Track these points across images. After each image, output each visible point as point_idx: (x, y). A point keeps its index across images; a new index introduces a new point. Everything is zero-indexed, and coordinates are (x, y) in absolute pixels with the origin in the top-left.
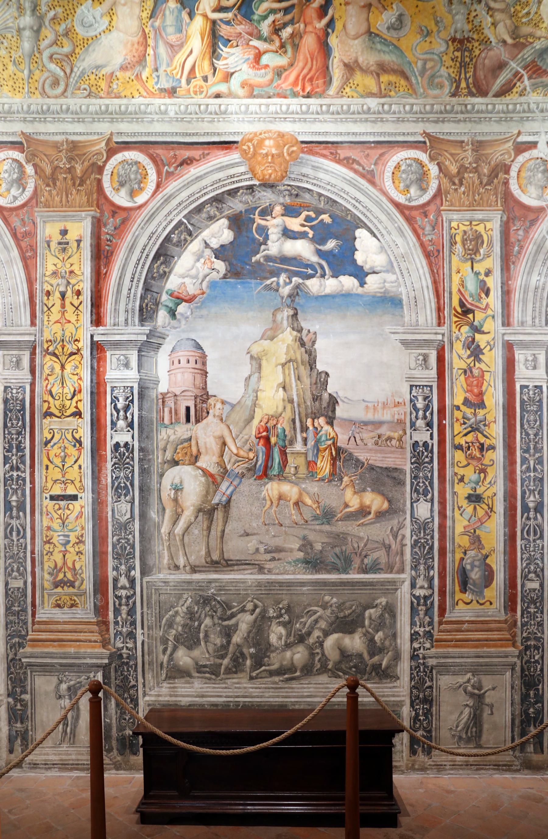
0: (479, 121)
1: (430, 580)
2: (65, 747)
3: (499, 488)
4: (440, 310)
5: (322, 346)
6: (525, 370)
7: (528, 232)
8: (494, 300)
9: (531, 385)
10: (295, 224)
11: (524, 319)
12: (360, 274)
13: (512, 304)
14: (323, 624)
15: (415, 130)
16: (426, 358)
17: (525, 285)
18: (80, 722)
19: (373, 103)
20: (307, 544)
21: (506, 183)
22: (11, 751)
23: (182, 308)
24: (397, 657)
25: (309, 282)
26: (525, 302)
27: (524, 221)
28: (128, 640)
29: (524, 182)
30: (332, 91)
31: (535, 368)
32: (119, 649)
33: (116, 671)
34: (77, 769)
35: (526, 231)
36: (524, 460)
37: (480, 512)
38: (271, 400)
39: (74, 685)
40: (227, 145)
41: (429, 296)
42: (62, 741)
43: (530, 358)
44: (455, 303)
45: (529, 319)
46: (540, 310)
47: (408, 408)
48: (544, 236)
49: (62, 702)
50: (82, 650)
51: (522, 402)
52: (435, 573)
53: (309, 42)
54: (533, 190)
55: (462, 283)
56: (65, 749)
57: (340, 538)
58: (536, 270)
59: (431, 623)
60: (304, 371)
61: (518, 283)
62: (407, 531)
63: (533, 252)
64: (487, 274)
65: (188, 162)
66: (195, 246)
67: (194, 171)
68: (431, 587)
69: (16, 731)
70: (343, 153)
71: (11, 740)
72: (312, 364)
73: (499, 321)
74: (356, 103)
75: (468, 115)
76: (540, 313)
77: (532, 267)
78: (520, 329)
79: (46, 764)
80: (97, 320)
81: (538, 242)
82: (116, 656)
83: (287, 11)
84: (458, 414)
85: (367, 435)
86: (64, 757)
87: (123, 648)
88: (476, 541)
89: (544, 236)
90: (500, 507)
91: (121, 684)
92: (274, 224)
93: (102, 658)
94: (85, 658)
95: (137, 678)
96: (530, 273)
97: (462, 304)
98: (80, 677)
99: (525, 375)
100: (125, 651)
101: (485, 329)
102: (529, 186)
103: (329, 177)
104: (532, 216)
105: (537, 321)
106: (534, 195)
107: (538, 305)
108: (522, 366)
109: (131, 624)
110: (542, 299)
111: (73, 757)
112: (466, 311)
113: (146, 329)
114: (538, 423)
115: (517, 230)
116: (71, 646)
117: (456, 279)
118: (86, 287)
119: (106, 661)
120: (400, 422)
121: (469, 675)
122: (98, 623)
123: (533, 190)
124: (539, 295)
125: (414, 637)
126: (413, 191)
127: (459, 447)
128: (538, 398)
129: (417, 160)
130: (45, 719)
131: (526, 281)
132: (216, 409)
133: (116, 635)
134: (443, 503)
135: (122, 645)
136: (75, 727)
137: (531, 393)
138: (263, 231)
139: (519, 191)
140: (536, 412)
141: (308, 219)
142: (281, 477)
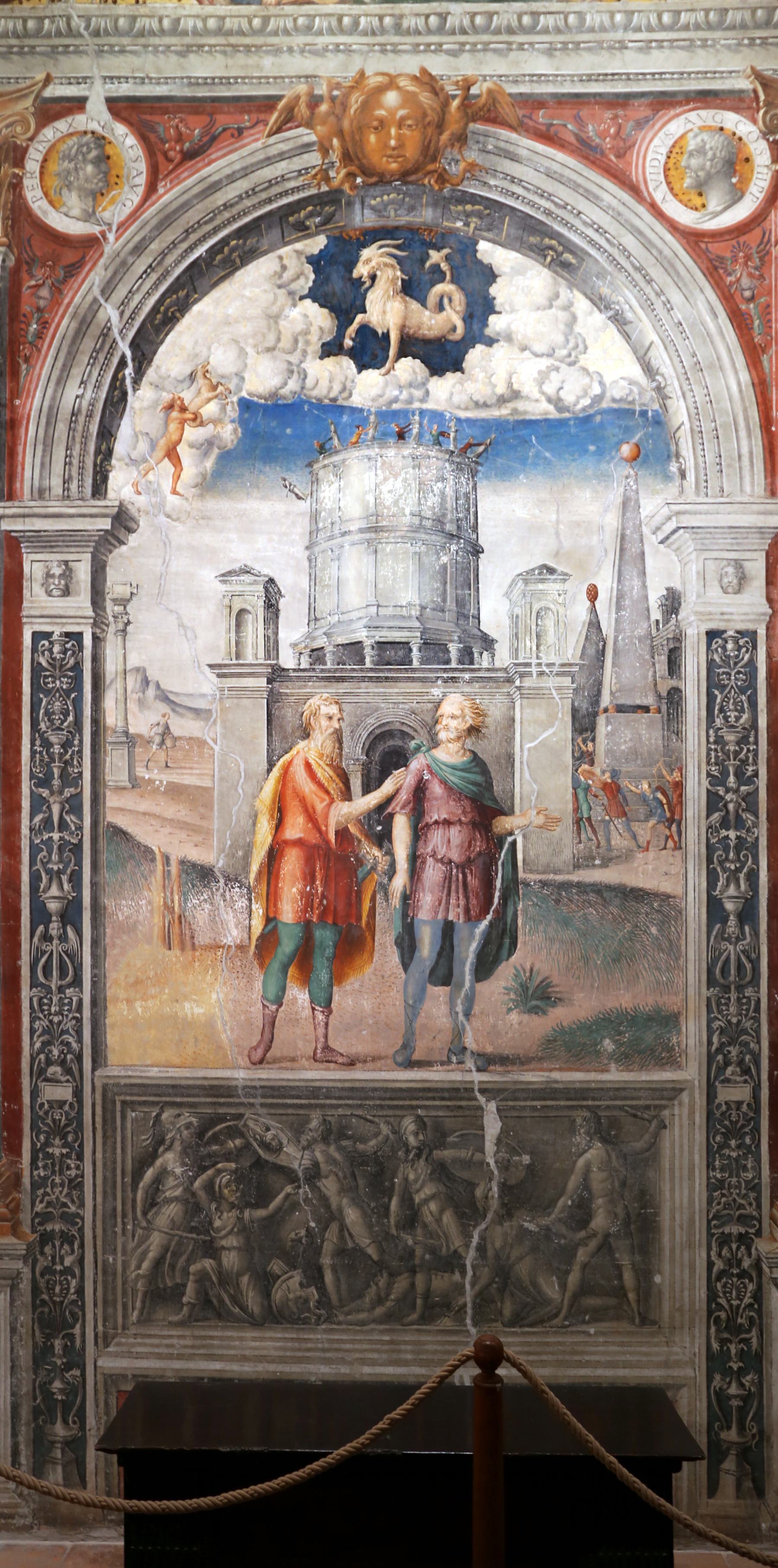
6: (43, 597)
7: (60, 291)
9: (57, 630)
11: (46, 483)
13: (20, 449)
17: (51, 408)
26: (48, 444)
27: (52, 268)
29: (53, 183)
31: (66, 592)
35: (57, 291)
36: (38, 803)
43: (57, 571)
45: (56, 483)
46: (82, 462)
48: (95, 300)
51: (36, 668)
54: (74, 202)
58: (77, 373)
63: (71, 333)
76: (82, 468)
77: (67, 369)
78: (37, 507)
81: (82, 312)
89: (95, 300)
96: (62, 382)
102: (65, 191)
104: (70, 257)
105: (74, 486)
106: (76, 212)
107: (76, 452)
108: (38, 589)
110: (85, 437)
114: (71, 718)
115: (38, 286)
124: (80, 428)
128: (72, 661)
131: (53, 398)
137: (56, 649)
139: (44, 204)
140: (68, 693)
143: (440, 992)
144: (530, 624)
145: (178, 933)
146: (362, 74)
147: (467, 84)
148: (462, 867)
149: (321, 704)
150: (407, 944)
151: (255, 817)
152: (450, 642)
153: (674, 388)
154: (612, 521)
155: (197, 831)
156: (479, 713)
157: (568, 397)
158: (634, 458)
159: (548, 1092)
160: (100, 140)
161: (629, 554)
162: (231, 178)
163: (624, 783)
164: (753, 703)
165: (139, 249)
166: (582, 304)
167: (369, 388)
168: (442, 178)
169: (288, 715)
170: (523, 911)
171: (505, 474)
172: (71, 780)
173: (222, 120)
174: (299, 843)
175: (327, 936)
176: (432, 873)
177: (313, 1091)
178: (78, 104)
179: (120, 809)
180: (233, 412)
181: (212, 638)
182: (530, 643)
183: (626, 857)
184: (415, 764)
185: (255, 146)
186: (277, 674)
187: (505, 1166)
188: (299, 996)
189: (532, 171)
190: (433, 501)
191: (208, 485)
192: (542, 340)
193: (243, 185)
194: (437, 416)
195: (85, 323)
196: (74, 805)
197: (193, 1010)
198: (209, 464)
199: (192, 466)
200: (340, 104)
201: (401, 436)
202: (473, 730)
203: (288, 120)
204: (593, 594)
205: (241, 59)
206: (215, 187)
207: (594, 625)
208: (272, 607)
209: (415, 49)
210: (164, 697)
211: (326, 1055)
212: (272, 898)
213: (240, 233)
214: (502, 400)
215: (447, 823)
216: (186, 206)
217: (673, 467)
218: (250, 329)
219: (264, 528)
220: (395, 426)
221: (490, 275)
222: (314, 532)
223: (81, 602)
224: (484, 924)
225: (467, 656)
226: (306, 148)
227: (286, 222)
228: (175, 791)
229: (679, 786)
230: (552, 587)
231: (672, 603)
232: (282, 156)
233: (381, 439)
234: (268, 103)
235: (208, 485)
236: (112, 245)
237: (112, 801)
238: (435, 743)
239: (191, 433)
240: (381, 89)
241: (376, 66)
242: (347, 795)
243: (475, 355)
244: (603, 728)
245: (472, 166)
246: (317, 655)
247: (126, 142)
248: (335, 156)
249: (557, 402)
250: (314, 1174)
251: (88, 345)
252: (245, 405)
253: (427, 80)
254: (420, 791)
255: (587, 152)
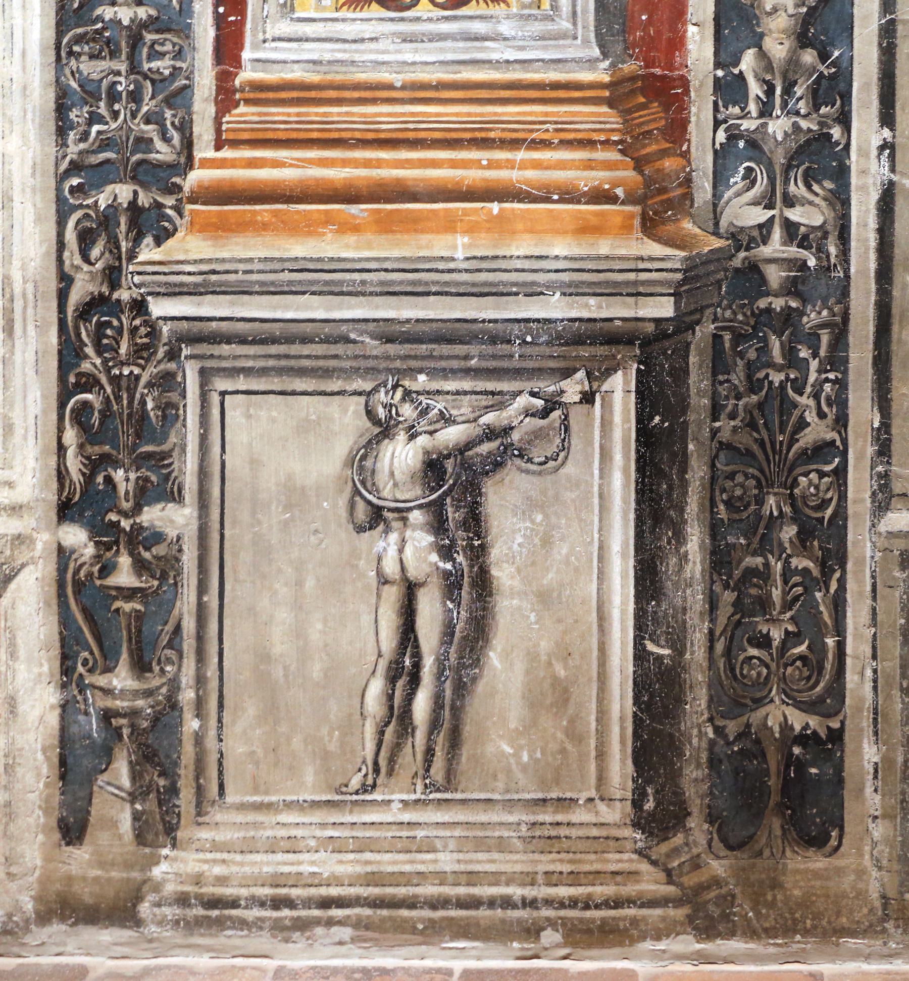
2: (393, 805)
18: (494, 658)
22: (72, 829)
28: (797, 189)
32: (741, 239)
33: (719, 364)
34: (464, 931)
39: (463, 449)
42: (382, 768)
49: (387, 545)
50: (521, 247)
56: (395, 814)
69: (107, 716)
71: (75, 765)
79: (278, 903)
82: (724, 280)
86: (389, 862)
87: (765, 229)
91: (745, 440)
93: (637, 293)
94: (533, 292)
95: (840, 402)
98: (499, 401)
100: (775, 246)
109: (817, 98)
111: (447, 861)
116: (450, 225)
119: (664, 308)
122: (617, 94)
130: (280, 644)
133: (723, 157)
135: (760, 215)
136: (462, 689)
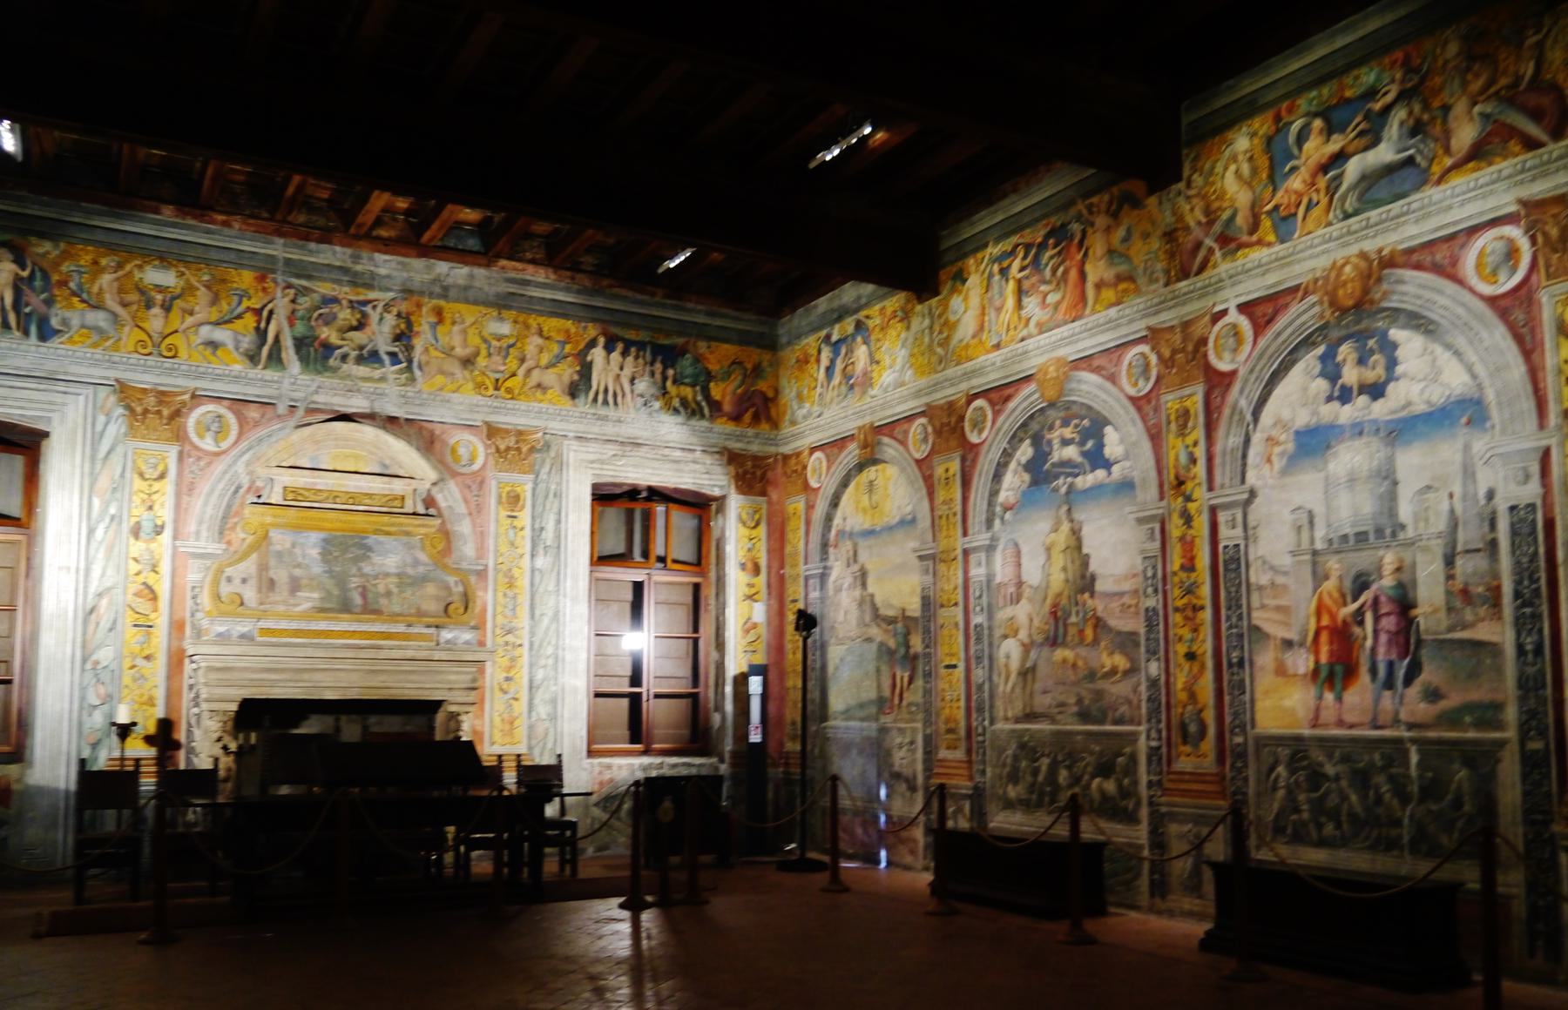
0: (1184, 303)
1: (1159, 732)
3: (1208, 646)
4: (1161, 486)
5: (1086, 532)
8: (1200, 470)
10: (1068, 433)
12: (1108, 465)
14: (1089, 769)
15: (1139, 327)
16: (1152, 530)
19: (1113, 312)
20: (1080, 701)
21: (1205, 355)
23: (1008, 516)
24: (1138, 804)
25: (1079, 479)
30: (1088, 311)
36: (1228, 618)
37: (1195, 670)
38: (1057, 580)
40: (1028, 379)
41: (1153, 474)
44: (1172, 476)
47: (1141, 578)
52: (1163, 725)
53: (1073, 274)
54: (1227, 356)
55: (1177, 459)
57: (1099, 694)
58: (1233, 431)
59: (1161, 773)
60: (1076, 555)
61: (1218, 448)
62: (1143, 688)
64: (1196, 444)
65: (1007, 399)
66: (1013, 465)
67: (1011, 405)
68: (1160, 739)
70: (1096, 363)
72: (1079, 547)
73: (1205, 487)
74: (1101, 317)
75: (1180, 300)
80: (965, 534)
83: (1059, 253)
84: (1176, 579)
85: (1115, 605)
88: (1192, 696)
90: (1210, 664)
92: (1055, 436)
97: (1177, 477)
99: (1228, 536)
101: (1195, 496)
103: (1088, 386)
112: (1180, 483)
113: (989, 535)
117: (1172, 454)
118: (958, 508)
120: (1136, 592)
121: (1190, 826)
123: (1227, 356)
125: (1150, 784)
126: (1141, 383)
127: (1177, 610)
129: (1143, 354)
132: (1027, 592)
134: (1167, 661)
138: (1050, 442)
141: (1076, 426)
142: (1064, 644)
143: (1387, 694)
144: (1421, 516)
145: (1281, 670)
146: (1334, 263)
147: (1380, 251)
148: (1397, 633)
149: (1333, 565)
150: (1373, 671)
151: (1308, 617)
152: (1387, 529)
153: (1486, 383)
154: (1458, 457)
155: (1287, 625)
156: (1401, 560)
157: (1434, 399)
158: (1468, 423)
159: (1440, 742)
160: (1235, 326)
161: (1468, 473)
162: (1286, 328)
163: (1471, 588)
164: (1535, 540)
165: (1251, 371)
166: (1439, 349)
167: (1346, 414)
168: (1372, 302)
169: (1320, 569)
170: (1425, 654)
171: (1408, 443)
172: (1240, 607)
173: (1281, 302)
174: (1326, 627)
175: (1338, 670)
176: (1383, 638)
177: (1336, 740)
178: (1224, 312)
179: (1259, 618)
180: (1292, 437)
181: (1287, 539)
182: (1422, 524)
183: (1472, 625)
184: (1374, 587)
185: (1294, 309)
186: (1315, 553)
187: (1421, 777)
188: (1329, 697)
189: (1412, 287)
190: (1375, 463)
191: (1285, 472)
192: (1424, 371)
193: (1289, 330)
194: (1375, 421)
195: (1234, 408)
196: (1240, 618)
197: (1288, 703)
198: (1284, 461)
199: (1278, 464)
200: (1326, 278)
201: (1361, 433)
202: (1398, 569)
203: (1306, 294)
204: (1451, 496)
205: (1286, 270)
206: (1279, 334)
207: (1452, 511)
208: (1311, 523)
209: (1357, 241)
210: (1272, 568)
211: (1340, 723)
212: (1317, 653)
213: (1291, 353)
214: (1404, 408)
215: (1388, 614)
216: (1268, 347)
217: (1488, 425)
218: (1299, 397)
219: (1307, 489)
220: (1358, 430)
221: (1395, 346)
222: (1327, 485)
223: (1239, 531)
224: (1406, 661)
225: (1394, 534)
226: (1313, 305)
227: (1307, 343)
228: (1279, 609)
229: (1498, 588)
230: (1431, 495)
231: (1490, 495)
232: (1305, 311)
233: (1353, 437)
234: (1296, 289)
235: (1285, 472)
236: (1242, 372)
237: (1255, 614)
238: (1381, 577)
239: (1277, 450)
240: (1344, 265)
241: (1340, 255)
242: (1345, 604)
243: (1391, 388)
244: (1459, 562)
245: (1385, 293)
246: (1330, 541)
247: (1244, 323)
248: (1326, 305)
249: (1428, 402)
250: (1337, 778)
251: (1236, 418)
252: (1297, 433)
253: (1363, 255)
254: (1376, 602)
255: (1437, 269)
